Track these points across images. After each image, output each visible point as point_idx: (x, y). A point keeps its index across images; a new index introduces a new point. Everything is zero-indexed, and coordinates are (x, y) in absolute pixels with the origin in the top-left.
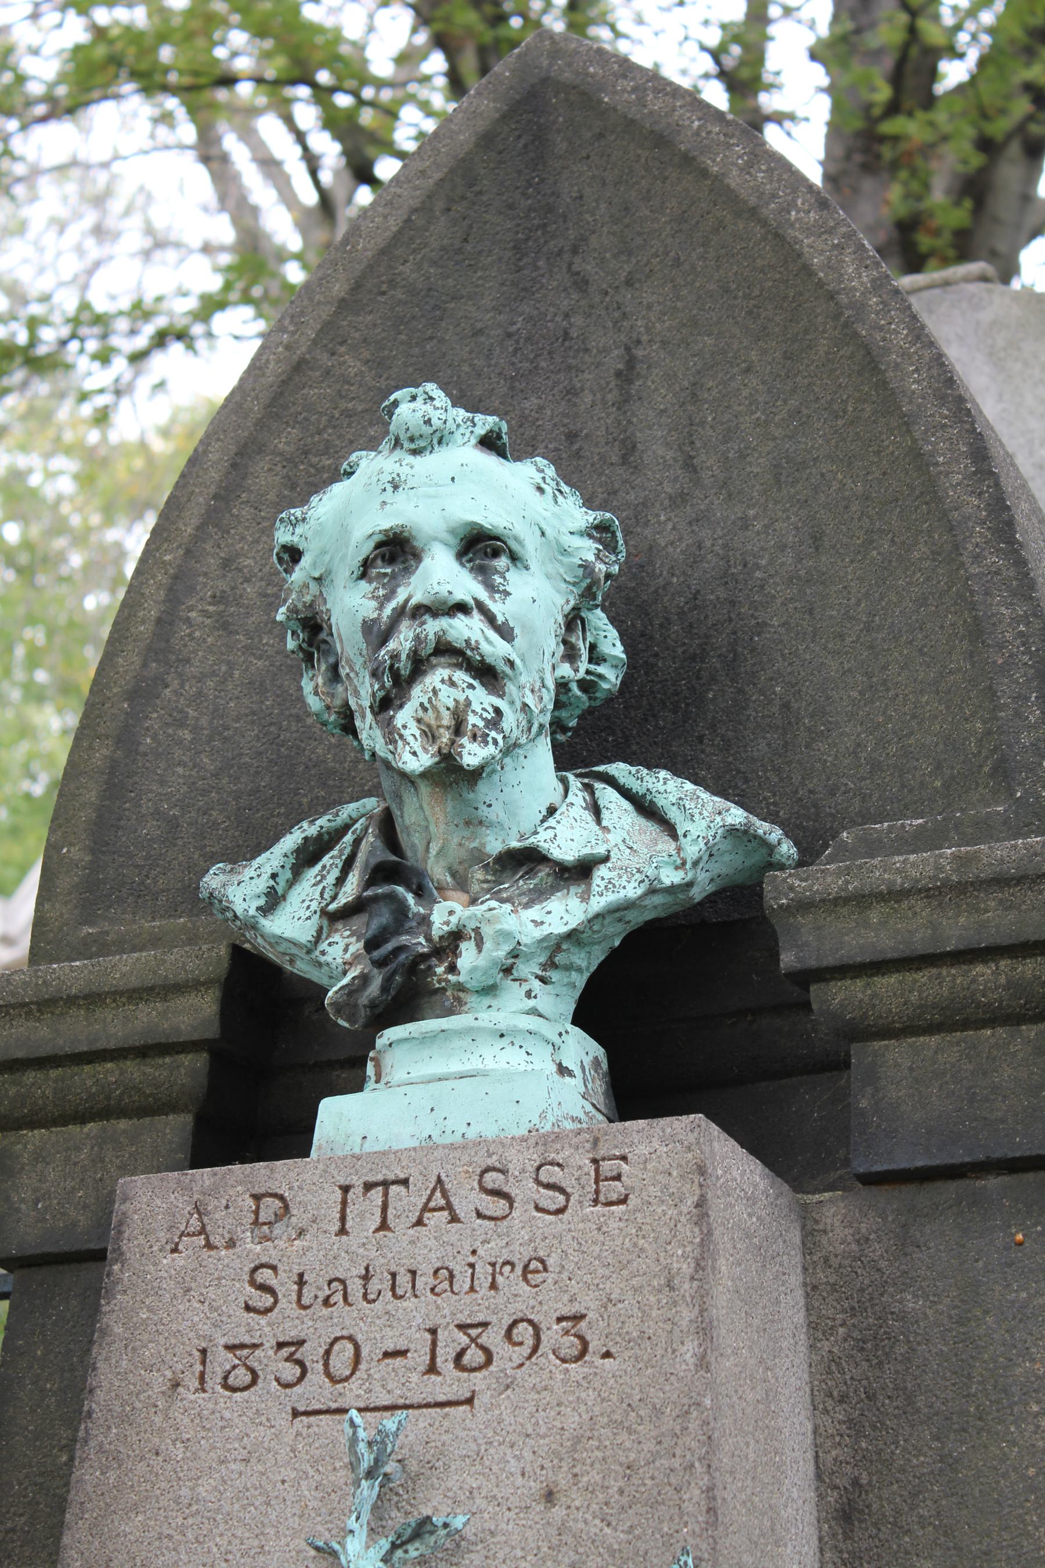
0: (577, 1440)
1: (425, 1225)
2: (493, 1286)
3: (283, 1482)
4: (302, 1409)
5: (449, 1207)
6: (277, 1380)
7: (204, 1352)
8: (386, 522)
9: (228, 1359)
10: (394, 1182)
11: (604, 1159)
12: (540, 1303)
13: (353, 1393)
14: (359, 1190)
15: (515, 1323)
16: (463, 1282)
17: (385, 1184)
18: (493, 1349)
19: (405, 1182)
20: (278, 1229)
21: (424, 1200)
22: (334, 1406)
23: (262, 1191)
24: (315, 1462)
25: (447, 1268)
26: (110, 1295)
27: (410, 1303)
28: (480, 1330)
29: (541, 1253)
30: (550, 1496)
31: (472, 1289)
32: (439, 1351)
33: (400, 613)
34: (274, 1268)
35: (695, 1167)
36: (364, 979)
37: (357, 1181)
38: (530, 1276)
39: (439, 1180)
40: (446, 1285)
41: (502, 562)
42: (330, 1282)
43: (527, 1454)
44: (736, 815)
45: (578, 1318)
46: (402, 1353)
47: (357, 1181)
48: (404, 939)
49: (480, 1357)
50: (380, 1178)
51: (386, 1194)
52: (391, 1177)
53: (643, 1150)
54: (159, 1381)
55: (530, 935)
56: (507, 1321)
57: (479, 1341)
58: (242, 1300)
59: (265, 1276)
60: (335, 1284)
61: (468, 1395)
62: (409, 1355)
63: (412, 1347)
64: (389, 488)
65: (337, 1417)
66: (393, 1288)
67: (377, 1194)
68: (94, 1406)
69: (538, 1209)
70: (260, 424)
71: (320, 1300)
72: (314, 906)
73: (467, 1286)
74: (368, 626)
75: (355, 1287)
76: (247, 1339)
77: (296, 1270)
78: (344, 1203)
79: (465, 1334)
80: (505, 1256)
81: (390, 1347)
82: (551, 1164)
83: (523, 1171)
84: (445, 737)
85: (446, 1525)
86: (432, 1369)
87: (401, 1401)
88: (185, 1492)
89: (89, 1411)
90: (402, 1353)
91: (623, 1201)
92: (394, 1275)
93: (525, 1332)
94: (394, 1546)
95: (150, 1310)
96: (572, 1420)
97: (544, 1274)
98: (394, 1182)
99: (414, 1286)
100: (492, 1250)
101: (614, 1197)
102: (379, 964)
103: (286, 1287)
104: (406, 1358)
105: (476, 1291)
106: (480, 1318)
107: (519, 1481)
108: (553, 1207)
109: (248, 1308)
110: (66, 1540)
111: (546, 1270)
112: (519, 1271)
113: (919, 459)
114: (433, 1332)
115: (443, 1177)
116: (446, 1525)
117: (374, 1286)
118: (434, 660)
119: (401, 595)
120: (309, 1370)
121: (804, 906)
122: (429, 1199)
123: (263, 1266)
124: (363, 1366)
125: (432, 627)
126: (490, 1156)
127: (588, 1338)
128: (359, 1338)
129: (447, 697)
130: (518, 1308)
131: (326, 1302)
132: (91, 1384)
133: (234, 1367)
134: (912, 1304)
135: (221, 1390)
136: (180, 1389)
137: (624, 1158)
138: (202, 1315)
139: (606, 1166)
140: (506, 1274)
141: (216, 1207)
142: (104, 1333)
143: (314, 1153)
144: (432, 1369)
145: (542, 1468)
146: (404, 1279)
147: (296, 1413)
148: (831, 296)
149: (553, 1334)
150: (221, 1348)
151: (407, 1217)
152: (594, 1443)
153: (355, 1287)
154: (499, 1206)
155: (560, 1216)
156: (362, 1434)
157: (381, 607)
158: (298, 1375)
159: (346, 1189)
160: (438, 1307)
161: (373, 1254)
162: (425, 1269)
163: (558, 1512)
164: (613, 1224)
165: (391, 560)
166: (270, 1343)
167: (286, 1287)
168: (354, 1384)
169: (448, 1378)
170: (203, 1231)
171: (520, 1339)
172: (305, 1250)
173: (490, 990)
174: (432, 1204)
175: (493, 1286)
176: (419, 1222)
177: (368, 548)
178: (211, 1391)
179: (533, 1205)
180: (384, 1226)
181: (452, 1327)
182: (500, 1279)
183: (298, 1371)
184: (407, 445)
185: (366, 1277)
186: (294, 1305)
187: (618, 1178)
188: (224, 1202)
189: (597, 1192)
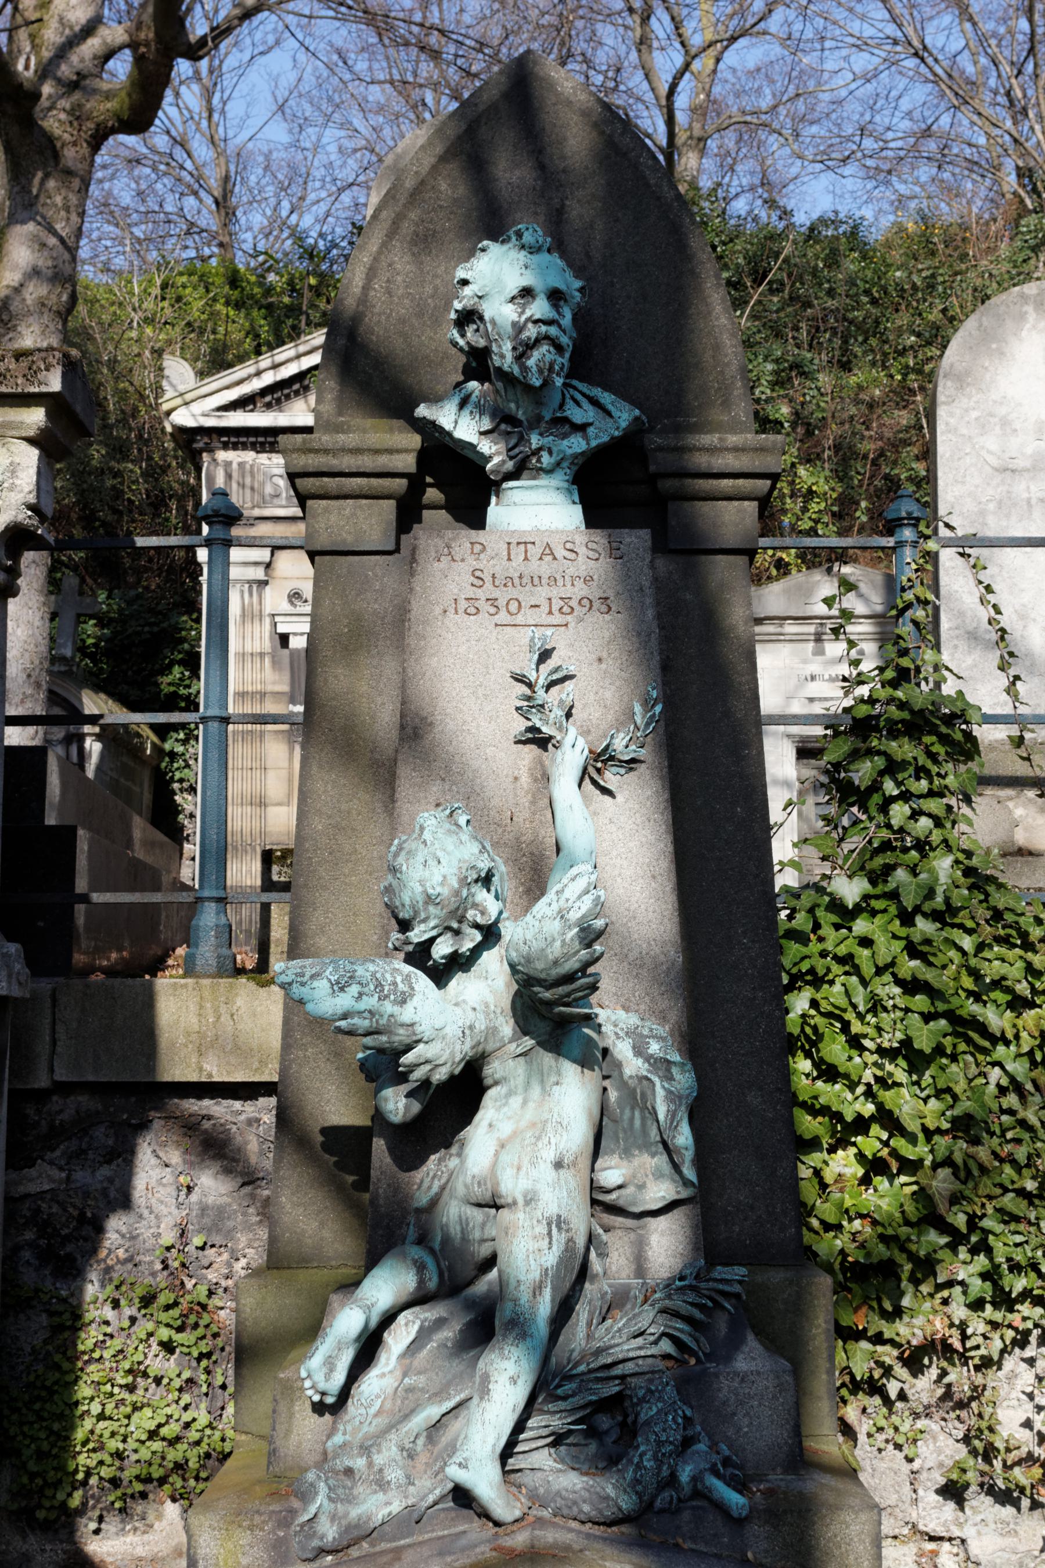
13: (520, 619)
16: (560, 582)
20: (482, 556)
27: (540, 588)
33: (528, 320)
36: (503, 462)
37: (514, 541)
41: (562, 303)
44: (637, 412)
45: (606, 599)
53: (628, 540)
54: (438, 610)
55: (570, 452)
59: (478, 573)
67: (522, 547)
70: (404, 205)
74: (514, 324)
75: (517, 581)
93: (585, 602)
100: (571, 571)
103: (488, 579)
117: (524, 581)
121: (660, 449)
144: (550, 613)
146: (536, 581)
148: (659, 198)
153: (517, 581)
154: (572, 556)
162: (545, 576)
163: (603, 666)
165: (522, 297)
166: (484, 598)
167: (488, 579)
168: (519, 616)
172: (494, 566)
177: (515, 292)
180: (526, 559)
185: (521, 577)
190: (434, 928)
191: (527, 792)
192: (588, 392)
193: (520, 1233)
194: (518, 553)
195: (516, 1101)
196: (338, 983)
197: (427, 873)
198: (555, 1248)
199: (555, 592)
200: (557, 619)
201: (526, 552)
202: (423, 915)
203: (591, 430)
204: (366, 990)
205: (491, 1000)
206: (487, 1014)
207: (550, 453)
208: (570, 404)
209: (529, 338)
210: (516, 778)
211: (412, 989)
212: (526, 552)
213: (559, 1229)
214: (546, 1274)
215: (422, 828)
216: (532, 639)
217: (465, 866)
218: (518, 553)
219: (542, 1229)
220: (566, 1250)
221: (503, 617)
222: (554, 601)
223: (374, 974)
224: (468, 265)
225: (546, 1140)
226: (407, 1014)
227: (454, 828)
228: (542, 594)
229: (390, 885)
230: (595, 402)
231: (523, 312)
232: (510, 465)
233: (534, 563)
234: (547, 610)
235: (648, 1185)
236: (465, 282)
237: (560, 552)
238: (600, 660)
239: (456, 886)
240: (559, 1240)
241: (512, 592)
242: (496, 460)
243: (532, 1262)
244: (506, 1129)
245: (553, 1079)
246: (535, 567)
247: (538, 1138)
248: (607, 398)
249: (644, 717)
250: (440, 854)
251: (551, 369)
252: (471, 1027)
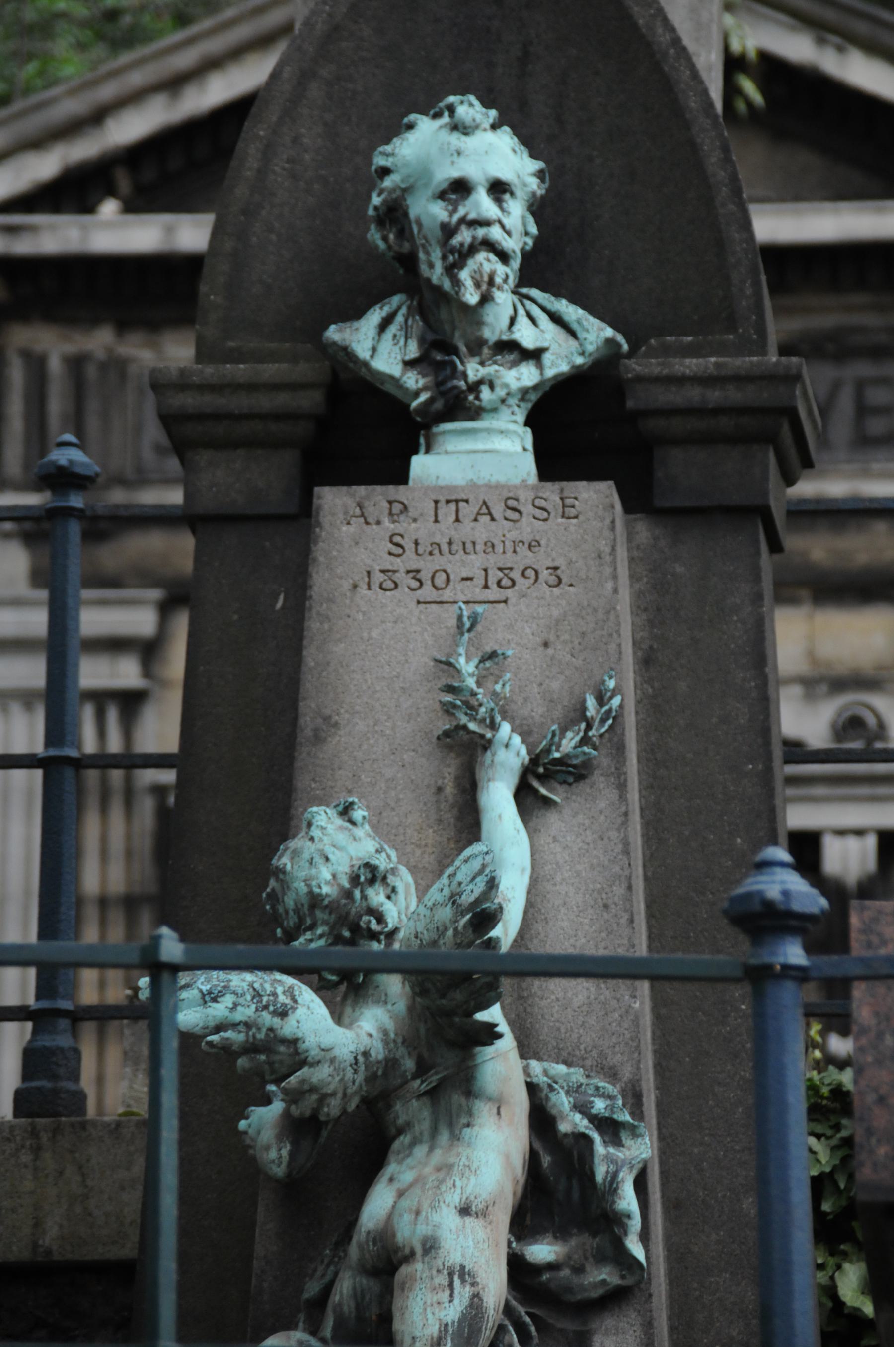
0: (558, 622)
2: (515, 551)
3: (415, 632)
5: (490, 514)
6: (409, 588)
7: (369, 573)
8: (455, 174)
9: (381, 577)
11: (566, 498)
13: (447, 595)
15: (526, 569)
16: (499, 548)
17: (457, 501)
18: (515, 579)
19: (467, 501)
20: (402, 518)
22: (438, 600)
24: (430, 624)
26: (316, 543)
27: (473, 557)
29: (538, 538)
30: (546, 645)
31: (504, 552)
33: (463, 220)
34: (402, 536)
37: (442, 499)
40: (490, 549)
41: (507, 196)
42: (431, 545)
43: (534, 626)
44: (609, 332)
45: (556, 568)
46: (471, 579)
47: (442, 499)
48: (455, 382)
49: (509, 583)
50: (454, 497)
52: (459, 497)
54: (346, 585)
55: (514, 385)
56: (522, 568)
58: (386, 550)
59: (397, 539)
60: (434, 546)
63: (476, 576)
64: (456, 154)
65: (440, 605)
66: (464, 549)
67: (453, 506)
69: (535, 518)
72: (399, 358)
73: (501, 551)
75: (445, 548)
76: (390, 568)
77: (414, 538)
78: (436, 509)
80: (520, 538)
81: (465, 575)
82: (541, 498)
83: (527, 500)
84: (484, 287)
85: (503, 654)
86: (486, 586)
88: (365, 635)
90: (471, 579)
91: (576, 517)
93: (530, 573)
94: (480, 661)
95: (339, 551)
96: (556, 613)
100: (513, 535)
101: (572, 515)
102: (443, 394)
103: (409, 546)
106: (509, 565)
107: (531, 637)
108: (541, 518)
109: (390, 554)
110: (305, 653)
111: (540, 545)
112: (527, 545)
113: (694, 147)
114: (486, 570)
115: (486, 500)
116: (503, 654)
118: (479, 247)
119: (461, 211)
121: (640, 379)
122: (480, 509)
124: (452, 583)
125: (481, 232)
126: (509, 491)
127: (562, 577)
128: (449, 571)
129: (487, 268)
130: (528, 562)
131: (431, 554)
133: (385, 580)
134: (679, 569)
136: (358, 589)
137: (576, 498)
139: (568, 501)
142: (315, 560)
143: (411, 482)
144: (486, 586)
145: (542, 632)
146: (469, 546)
147: (419, 602)
149: (545, 574)
152: (566, 623)
153: (445, 548)
154: (515, 516)
156: (465, 613)
157: (451, 215)
159: (436, 502)
163: (550, 651)
166: (403, 570)
167: (409, 546)
170: (362, 515)
172: (417, 529)
173: (495, 410)
174: (482, 512)
175: (515, 551)
177: (445, 185)
179: (531, 517)
180: (457, 520)
181: (495, 569)
182: (518, 549)
183: (418, 584)
184: (461, 129)
185: (450, 543)
187: (573, 507)
189: (564, 512)
190: (321, 937)
191: (453, 806)
192: (549, 306)
193: (417, 1286)
194: (447, 513)
195: (420, 1151)
196: (210, 993)
197: (314, 871)
198: (456, 1301)
199: (493, 561)
200: (494, 593)
201: (457, 511)
202: (309, 921)
203: (547, 358)
204: (241, 1000)
205: (390, 1025)
206: (386, 1042)
207: (492, 387)
208: (523, 321)
209: (462, 244)
210: (440, 790)
211: (295, 1001)
212: (457, 511)
213: (463, 1281)
214: (446, 1330)
215: (310, 825)
216: (460, 618)
217: (357, 863)
218: (447, 513)
219: (443, 1280)
220: (471, 1305)
221: (427, 592)
222: (490, 572)
223: (251, 985)
224: (388, 148)
225: (450, 1183)
226: (288, 1028)
227: (348, 825)
228: (474, 563)
229: (273, 890)
230: (556, 318)
231: (455, 210)
232: (439, 405)
233: (467, 524)
234: (482, 582)
235: (588, 1268)
236: (385, 172)
237: (498, 510)
238: (546, 645)
239: (347, 885)
240: (463, 1293)
241: (438, 562)
242: (423, 397)
243: (430, 1316)
244: (407, 1177)
245: (464, 1121)
246: (467, 531)
247: (442, 1182)
248: (571, 312)
249: (598, 712)
250: (330, 851)
251: (491, 282)
252: (366, 1054)
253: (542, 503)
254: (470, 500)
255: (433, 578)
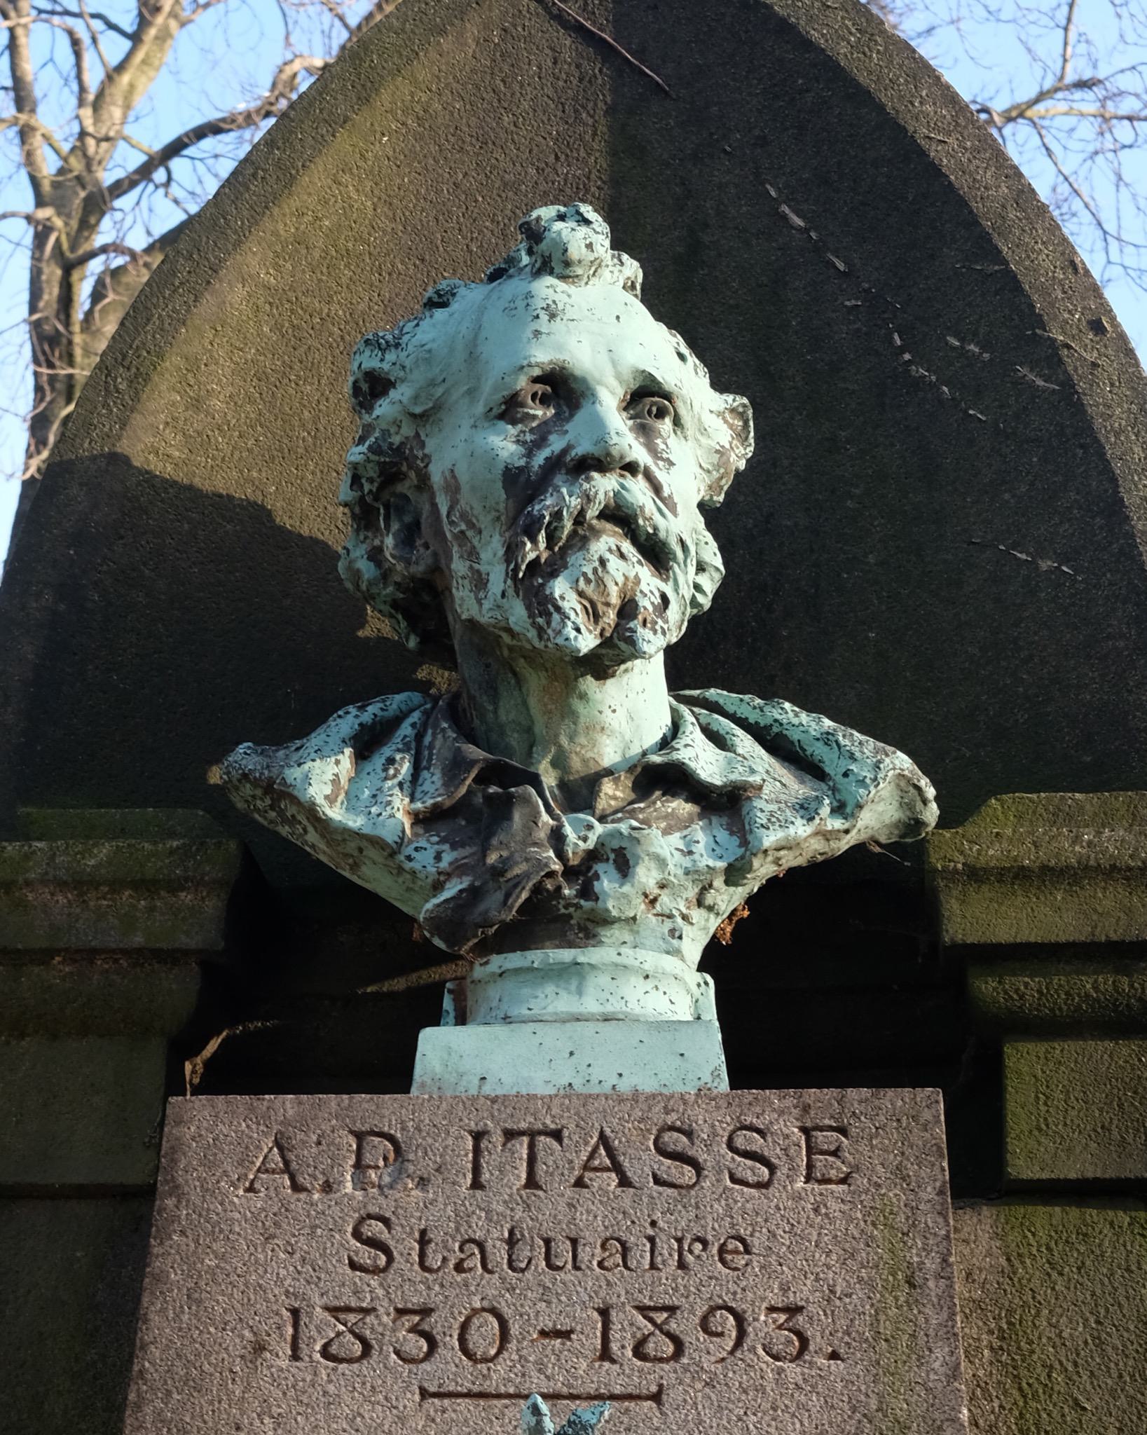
1: (587, 1187)
2: (682, 1265)
4: (432, 1389)
5: (617, 1168)
6: (397, 1353)
10: (540, 1133)
12: (744, 1290)
14: (498, 1138)
21: (584, 1156)
23: (366, 1128)
25: (618, 1240)
27: (569, 1276)
28: (665, 1315)
32: (615, 1335)
34: (386, 1221)
35: (934, 1148)
38: (729, 1257)
39: (603, 1138)
46: (565, 1335)
50: (523, 1125)
51: (532, 1147)
54: (235, 1343)
57: (666, 1327)
61: (654, 1389)
62: (573, 1336)
68: (147, 1364)
71: (451, 1264)
75: (499, 1254)
79: (645, 1317)
87: (565, 1390)
89: (140, 1371)
90: (565, 1335)
92: (547, 1242)
97: (747, 1257)
98: (540, 1133)
99: (575, 1257)
104: (570, 1339)
105: (658, 1269)
109: (353, 1265)
111: (747, 1251)
115: (608, 1131)
117: (523, 1253)
120: (441, 1344)
122: (592, 1156)
123: (370, 1216)
124: (513, 1345)
128: (507, 1312)
131: (459, 1268)
132: (142, 1339)
135: (322, 1360)
137: (843, 1131)
138: (291, 1269)
140: (697, 1252)
141: (304, 1142)
144: (605, 1354)
146: (564, 1251)
150: (318, 1309)
151: (562, 1174)
153: (499, 1254)
155: (764, 1191)
158: (425, 1348)
160: (609, 1284)
161: (519, 1214)
164: (834, 1205)
169: (626, 1367)
171: (720, 1329)
175: (682, 1265)
176: (580, 1183)
178: (307, 1359)
182: (690, 1258)
186: (416, 1267)
188: (314, 1138)
189: (810, 1166)
253: (756, 1143)
254: (566, 1133)
255: (464, 1327)
